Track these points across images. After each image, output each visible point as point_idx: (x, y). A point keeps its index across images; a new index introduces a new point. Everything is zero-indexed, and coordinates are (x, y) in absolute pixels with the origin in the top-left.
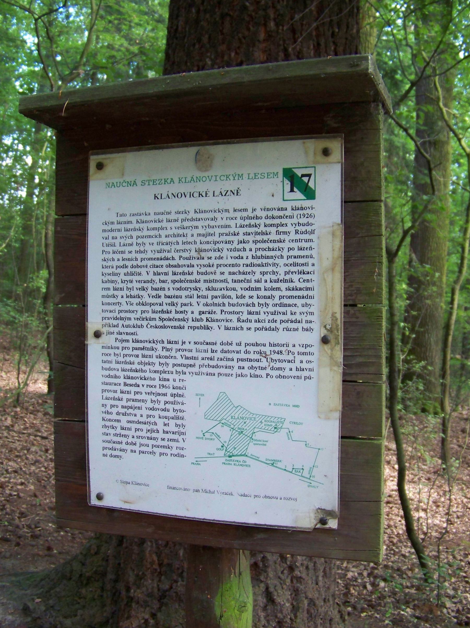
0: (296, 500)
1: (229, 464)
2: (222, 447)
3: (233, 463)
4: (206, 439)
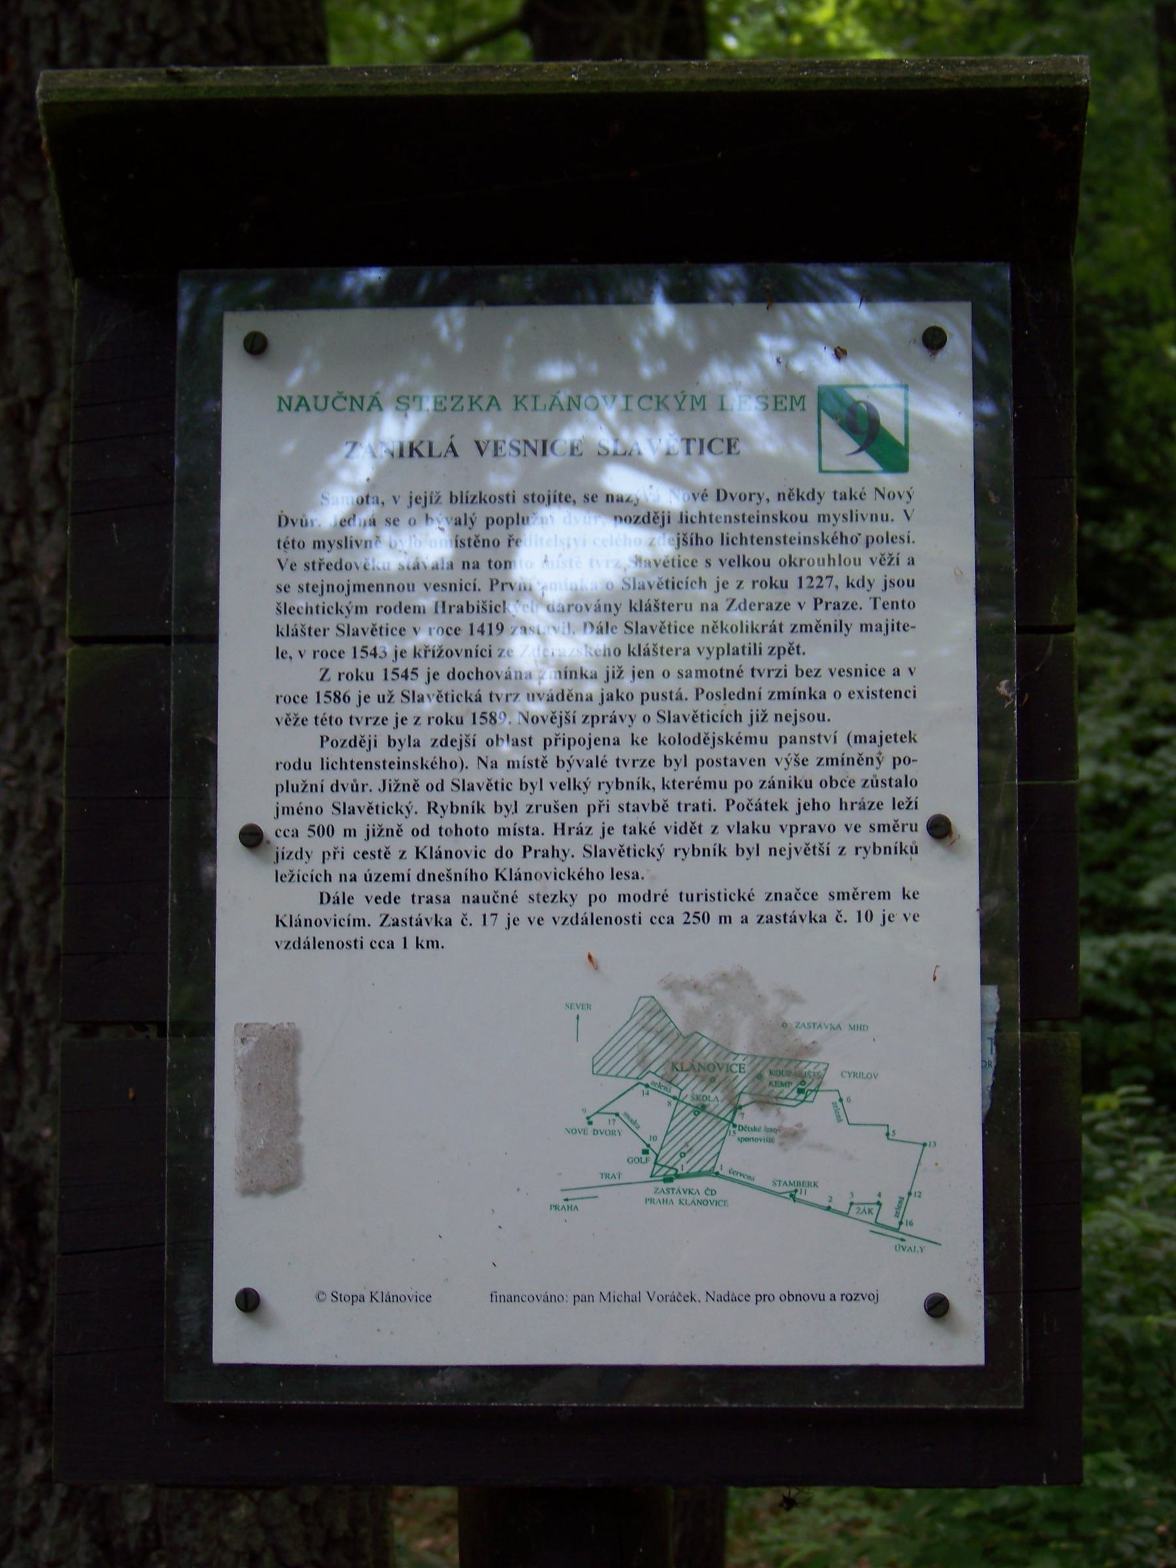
0: (874, 1298)
1: (665, 1201)
2: (645, 1152)
3: (675, 1198)
4: (595, 1132)
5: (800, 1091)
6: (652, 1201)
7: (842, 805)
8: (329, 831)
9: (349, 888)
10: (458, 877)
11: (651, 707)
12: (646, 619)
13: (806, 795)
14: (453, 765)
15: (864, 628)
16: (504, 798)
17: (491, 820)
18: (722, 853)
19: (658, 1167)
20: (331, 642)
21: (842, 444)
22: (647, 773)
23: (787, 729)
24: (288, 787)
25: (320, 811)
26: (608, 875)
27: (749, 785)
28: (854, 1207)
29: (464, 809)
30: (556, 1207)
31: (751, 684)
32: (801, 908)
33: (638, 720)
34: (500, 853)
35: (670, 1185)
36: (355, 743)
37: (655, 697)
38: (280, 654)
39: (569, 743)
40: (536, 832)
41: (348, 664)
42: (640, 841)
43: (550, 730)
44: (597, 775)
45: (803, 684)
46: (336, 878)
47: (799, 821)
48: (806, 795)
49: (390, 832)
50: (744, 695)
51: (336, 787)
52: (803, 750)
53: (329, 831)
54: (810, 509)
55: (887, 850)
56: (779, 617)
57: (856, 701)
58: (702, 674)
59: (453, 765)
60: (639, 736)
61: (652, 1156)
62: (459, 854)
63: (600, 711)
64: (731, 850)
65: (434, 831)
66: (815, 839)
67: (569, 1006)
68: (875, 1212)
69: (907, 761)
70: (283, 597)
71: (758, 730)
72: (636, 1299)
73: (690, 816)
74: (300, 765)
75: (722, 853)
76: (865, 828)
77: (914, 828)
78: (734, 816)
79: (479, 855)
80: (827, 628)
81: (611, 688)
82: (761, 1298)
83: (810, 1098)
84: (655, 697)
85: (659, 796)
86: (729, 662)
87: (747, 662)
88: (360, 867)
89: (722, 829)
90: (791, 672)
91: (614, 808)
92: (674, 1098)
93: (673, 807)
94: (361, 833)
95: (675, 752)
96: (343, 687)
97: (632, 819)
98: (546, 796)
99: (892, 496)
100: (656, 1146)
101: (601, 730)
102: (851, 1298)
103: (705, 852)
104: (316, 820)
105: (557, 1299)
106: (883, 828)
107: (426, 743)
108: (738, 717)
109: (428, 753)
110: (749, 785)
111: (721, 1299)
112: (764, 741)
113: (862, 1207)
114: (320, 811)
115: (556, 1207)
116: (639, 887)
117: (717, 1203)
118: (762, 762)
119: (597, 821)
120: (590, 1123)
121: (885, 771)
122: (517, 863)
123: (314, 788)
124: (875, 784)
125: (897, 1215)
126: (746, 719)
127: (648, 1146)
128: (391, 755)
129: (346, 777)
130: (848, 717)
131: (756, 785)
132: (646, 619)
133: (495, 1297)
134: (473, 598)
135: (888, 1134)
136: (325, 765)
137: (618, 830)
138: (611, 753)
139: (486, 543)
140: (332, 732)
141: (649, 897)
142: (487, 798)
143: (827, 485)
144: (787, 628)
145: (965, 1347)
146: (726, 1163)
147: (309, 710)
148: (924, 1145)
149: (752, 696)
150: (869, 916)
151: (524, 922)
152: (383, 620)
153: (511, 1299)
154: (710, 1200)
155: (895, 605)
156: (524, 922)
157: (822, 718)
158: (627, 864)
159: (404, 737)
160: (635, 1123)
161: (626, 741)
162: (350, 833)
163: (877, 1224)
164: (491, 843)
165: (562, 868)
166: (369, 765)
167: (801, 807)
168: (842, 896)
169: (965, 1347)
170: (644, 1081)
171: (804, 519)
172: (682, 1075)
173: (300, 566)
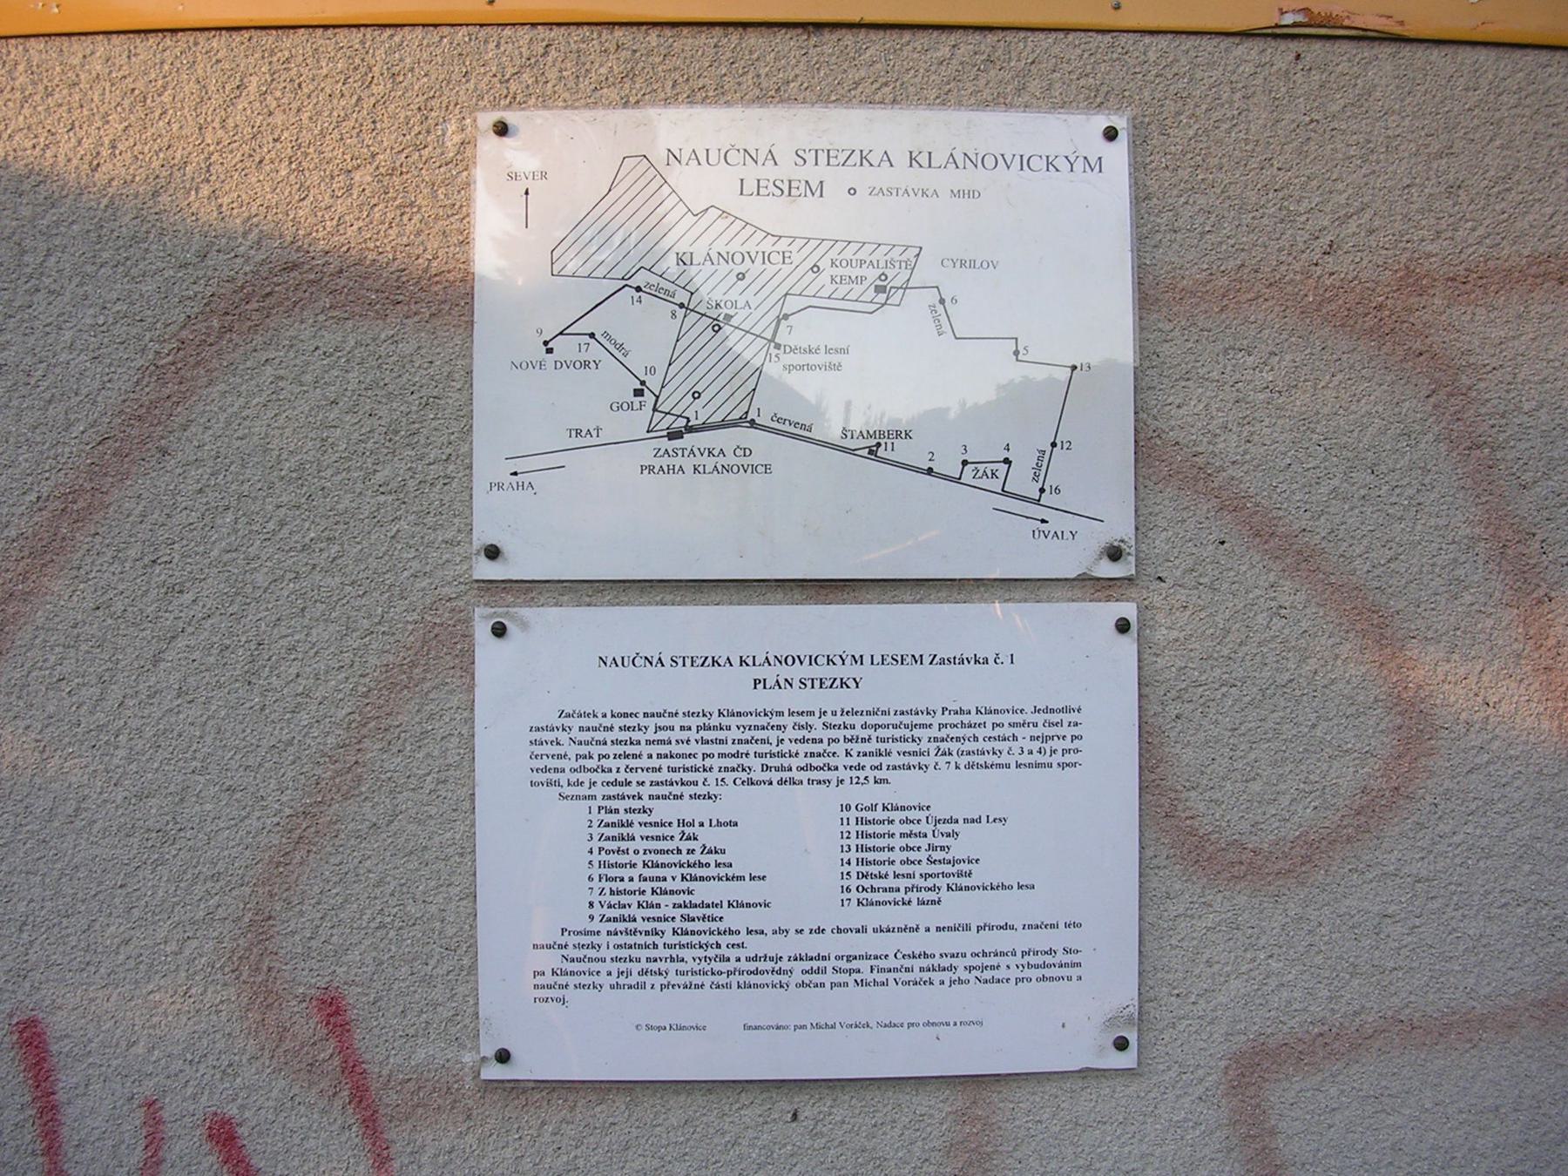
1: (671, 469)
2: (638, 393)
3: (688, 463)
5: (880, 289)
6: (651, 469)
19: (658, 416)
28: (969, 468)
35: (677, 443)
68: (1002, 475)
83: (895, 299)
92: (681, 306)
100: (654, 383)
113: (981, 467)
115: (500, 486)
117: (754, 469)
120: (550, 351)
125: (1035, 478)
127: (643, 383)
135: (1016, 353)
148: (1074, 368)
160: (620, 347)
163: (1004, 493)
170: (634, 282)
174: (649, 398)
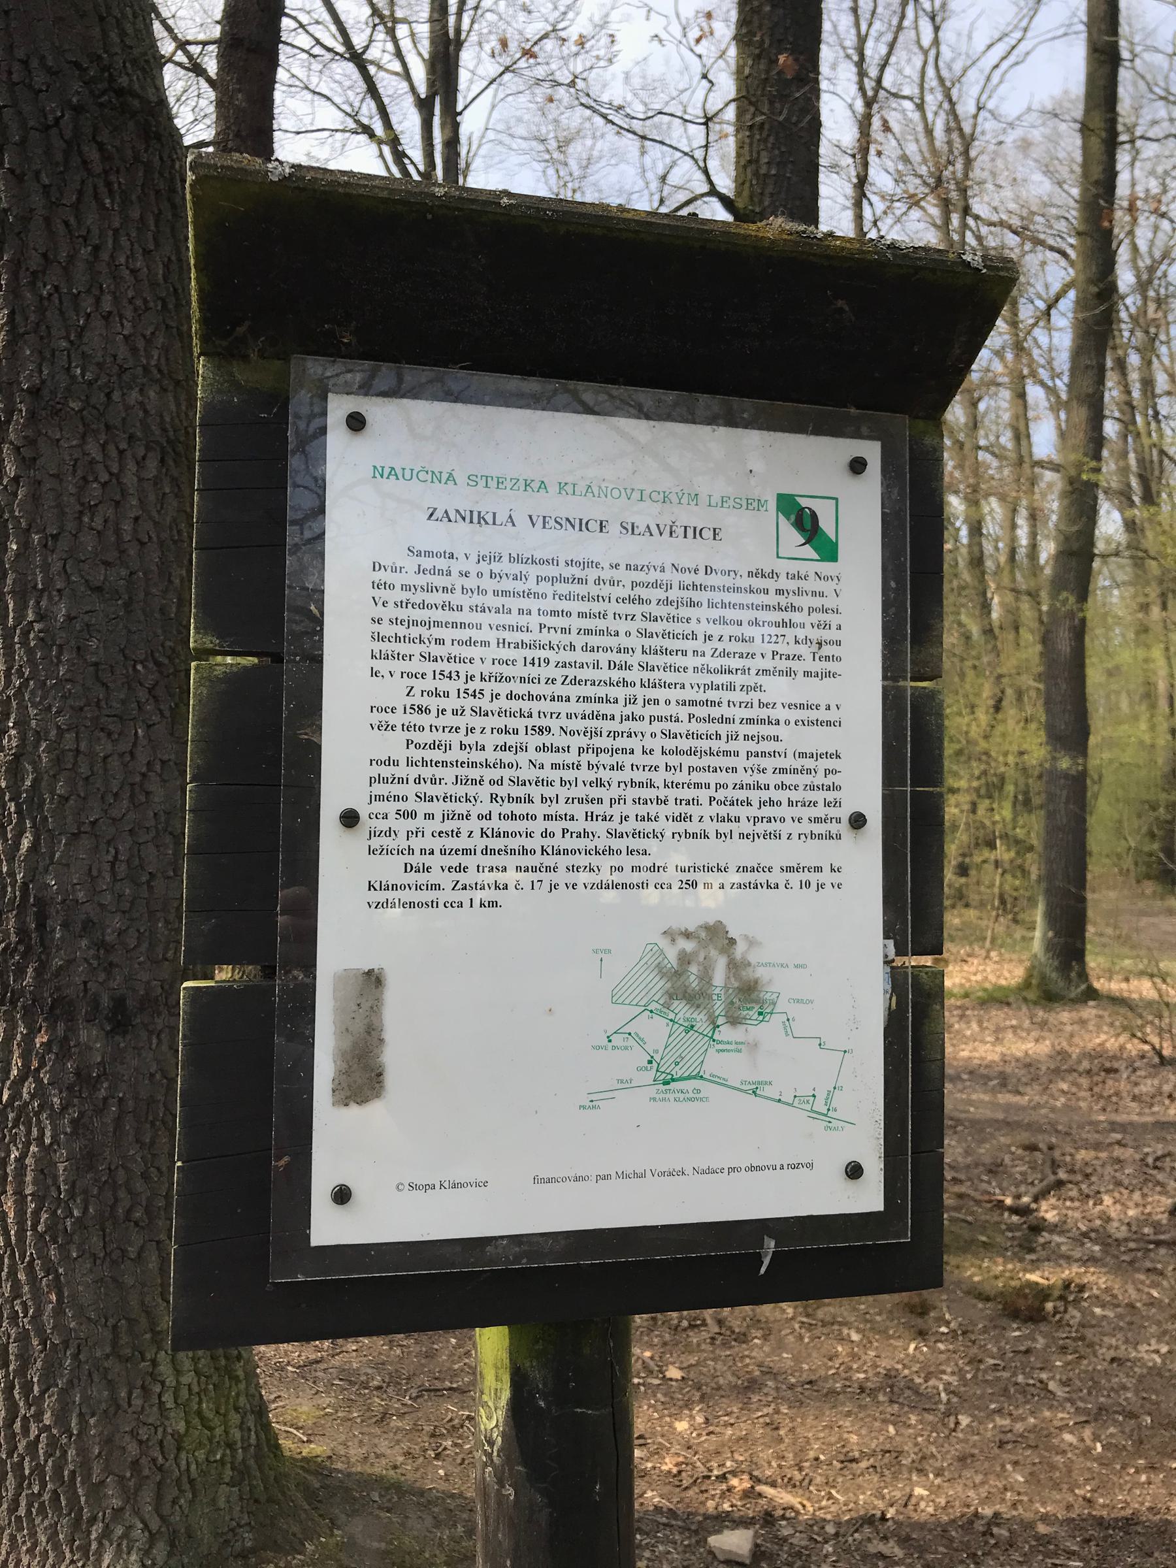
0: (810, 1166)
1: (664, 1100)
2: (650, 1062)
3: (671, 1096)
4: (614, 1048)
5: (760, 1014)
7: (790, 803)
8: (412, 815)
9: (428, 860)
10: (513, 852)
11: (657, 727)
12: (653, 660)
13: (765, 795)
14: (510, 766)
15: (807, 674)
16: (549, 792)
17: (539, 809)
18: (707, 837)
20: (415, 666)
21: (792, 537)
22: (653, 775)
23: (752, 746)
24: (380, 779)
25: (405, 799)
26: (624, 851)
27: (725, 786)
29: (518, 800)
30: (584, 1107)
31: (728, 712)
32: (761, 877)
33: (648, 735)
34: (545, 834)
36: (434, 746)
37: (660, 719)
38: (374, 673)
39: (598, 751)
40: (572, 819)
41: (429, 684)
42: (648, 827)
43: (583, 741)
44: (617, 776)
45: (764, 713)
46: (417, 852)
47: (760, 814)
48: (765, 795)
49: (461, 817)
50: (723, 720)
51: (418, 780)
52: (765, 762)
53: (412, 815)
54: (770, 584)
55: (820, 836)
56: (747, 663)
57: (800, 727)
58: (693, 703)
59: (510, 766)
60: (648, 747)
61: (655, 1065)
62: (514, 834)
63: (620, 728)
64: (712, 835)
65: (495, 816)
66: (771, 827)
67: (595, 951)
69: (834, 772)
70: (376, 627)
71: (732, 746)
72: (643, 1176)
73: (684, 809)
74: (389, 762)
75: (707, 837)
76: (805, 820)
77: (839, 821)
78: (715, 809)
79: (529, 835)
80: (781, 673)
81: (628, 711)
82: (732, 1170)
84: (660, 719)
85: (662, 793)
86: (713, 695)
87: (726, 696)
88: (437, 844)
89: (706, 819)
90: (756, 704)
91: (629, 801)
93: (672, 801)
94: (438, 817)
95: (673, 760)
96: (425, 701)
97: (642, 810)
98: (580, 791)
99: (826, 578)
100: (657, 1058)
101: (620, 743)
102: (795, 1167)
103: (694, 836)
104: (402, 806)
105: (584, 1179)
106: (817, 820)
107: (489, 748)
108: (718, 736)
109: (491, 756)
110: (725, 786)
111: (704, 1172)
112: (737, 754)
114: (405, 799)
115: (584, 1107)
116: (645, 861)
118: (734, 770)
119: (616, 810)
121: (819, 779)
122: (558, 842)
123: (401, 781)
124: (812, 788)
126: (724, 738)
128: (463, 756)
129: (427, 772)
130: (793, 739)
131: (731, 786)
132: (653, 660)
133: (536, 1180)
134: (527, 638)
136: (410, 763)
137: (632, 818)
138: (627, 760)
139: (536, 595)
140: (417, 737)
141: (654, 868)
142: (536, 792)
143: (783, 567)
144: (753, 672)
145: (869, 1197)
146: (708, 1069)
147: (397, 719)
149: (728, 721)
150: (808, 884)
151: (562, 887)
152: (456, 650)
153: (549, 1181)
154: (696, 1097)
155: (827, 658)
156: (562, 887)
157: (776, 739)
158: (635, 844)
159: (473, 742)
161: (638, 751)
162: (429, 816)
163: (812, 1111)
164: (538, 826)
165: (591, 846)
166: (444, 764)
167: (762, 804)
168: (790, 869)
169: (869, 1197)
171: (766, 592)
172: (676, 1003)
173: (391, 605)
174: (655, 1065)
